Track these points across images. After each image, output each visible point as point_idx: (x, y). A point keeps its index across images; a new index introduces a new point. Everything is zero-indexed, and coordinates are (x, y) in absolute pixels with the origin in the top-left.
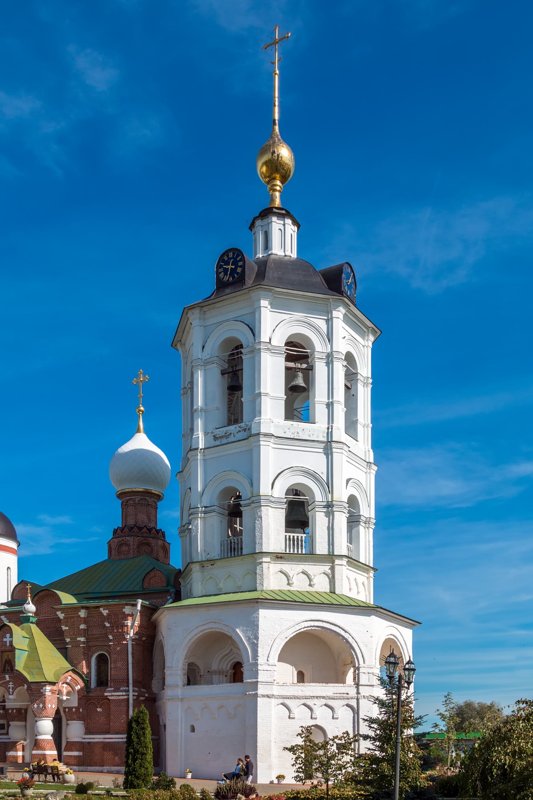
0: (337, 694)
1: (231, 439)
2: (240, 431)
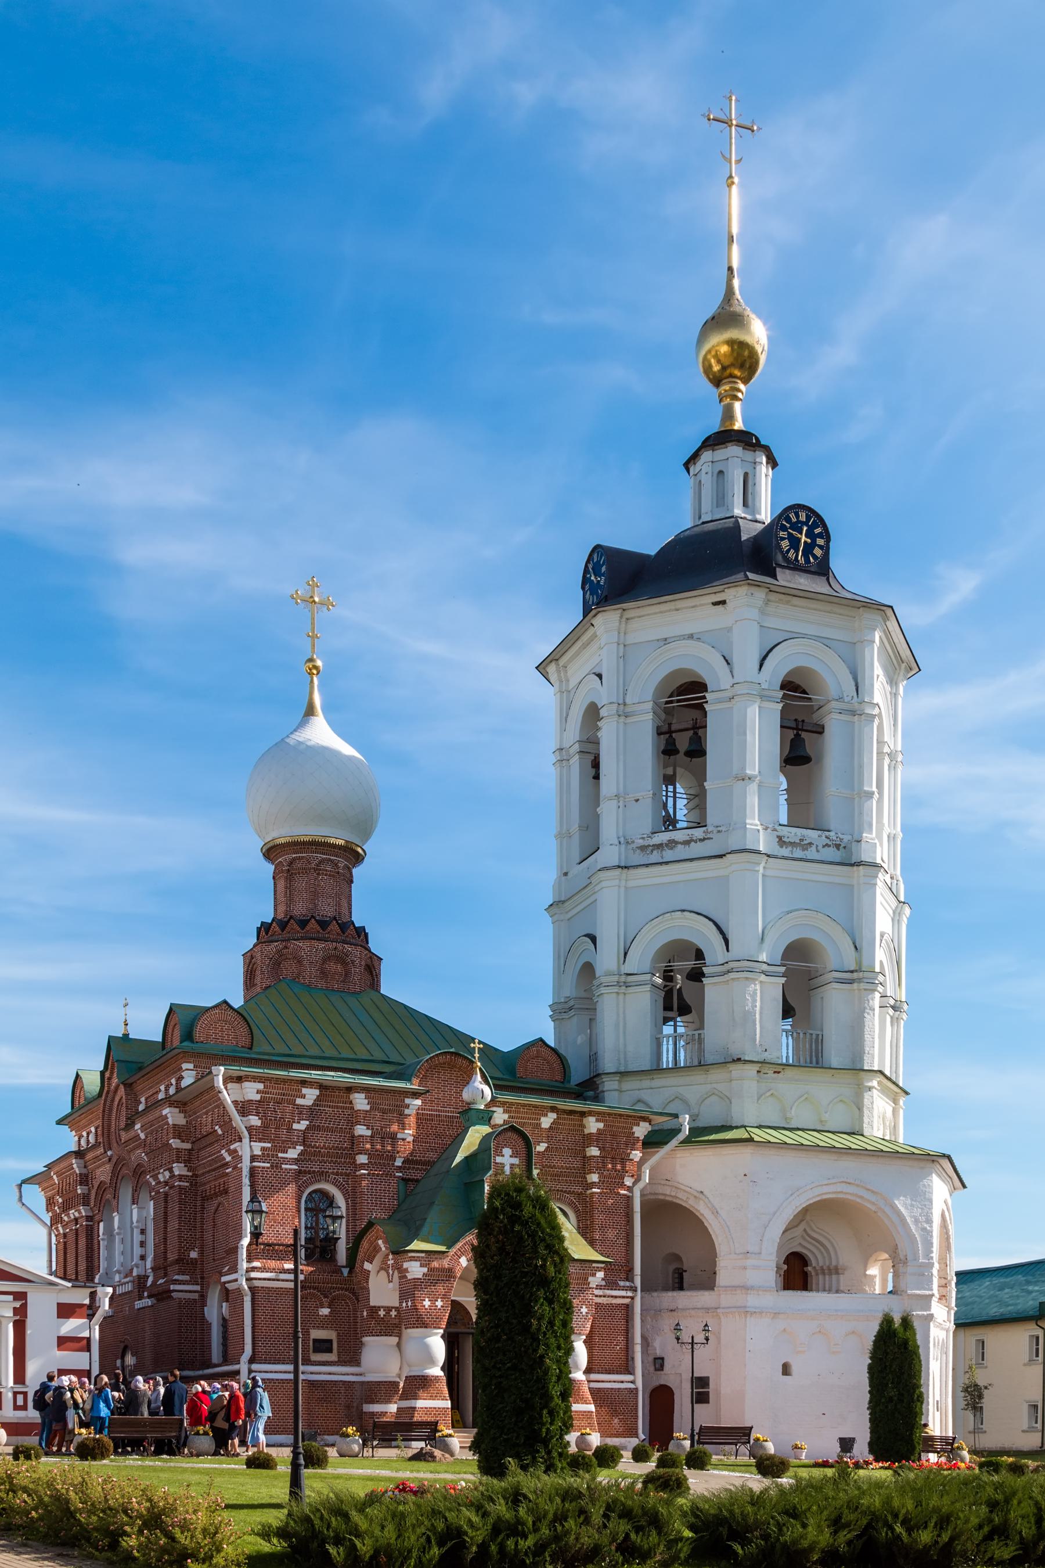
1: (812, 853)
2: (827, 845)
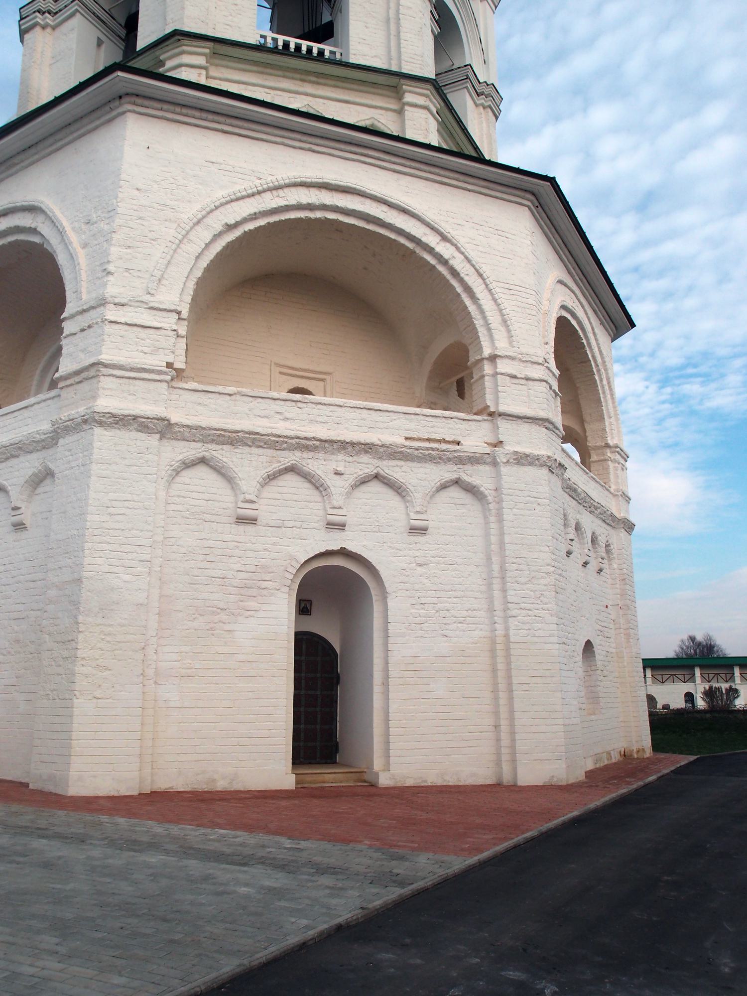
0: (420, 439)
